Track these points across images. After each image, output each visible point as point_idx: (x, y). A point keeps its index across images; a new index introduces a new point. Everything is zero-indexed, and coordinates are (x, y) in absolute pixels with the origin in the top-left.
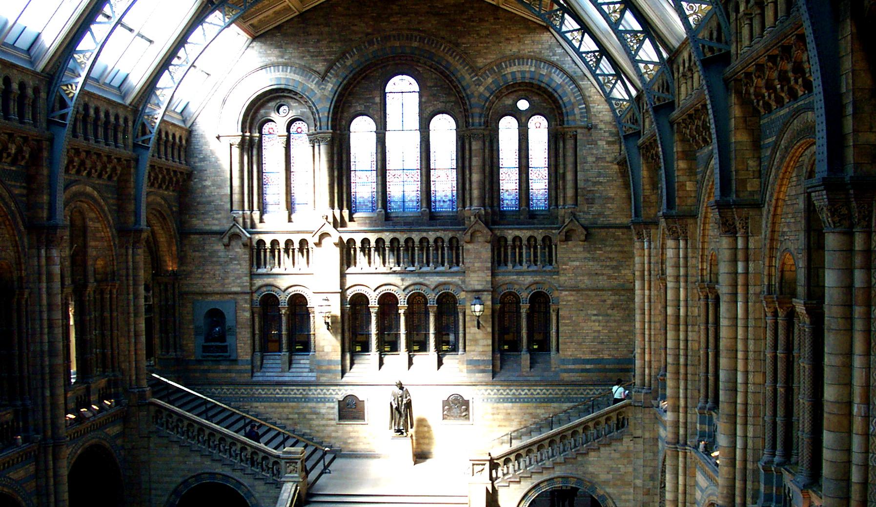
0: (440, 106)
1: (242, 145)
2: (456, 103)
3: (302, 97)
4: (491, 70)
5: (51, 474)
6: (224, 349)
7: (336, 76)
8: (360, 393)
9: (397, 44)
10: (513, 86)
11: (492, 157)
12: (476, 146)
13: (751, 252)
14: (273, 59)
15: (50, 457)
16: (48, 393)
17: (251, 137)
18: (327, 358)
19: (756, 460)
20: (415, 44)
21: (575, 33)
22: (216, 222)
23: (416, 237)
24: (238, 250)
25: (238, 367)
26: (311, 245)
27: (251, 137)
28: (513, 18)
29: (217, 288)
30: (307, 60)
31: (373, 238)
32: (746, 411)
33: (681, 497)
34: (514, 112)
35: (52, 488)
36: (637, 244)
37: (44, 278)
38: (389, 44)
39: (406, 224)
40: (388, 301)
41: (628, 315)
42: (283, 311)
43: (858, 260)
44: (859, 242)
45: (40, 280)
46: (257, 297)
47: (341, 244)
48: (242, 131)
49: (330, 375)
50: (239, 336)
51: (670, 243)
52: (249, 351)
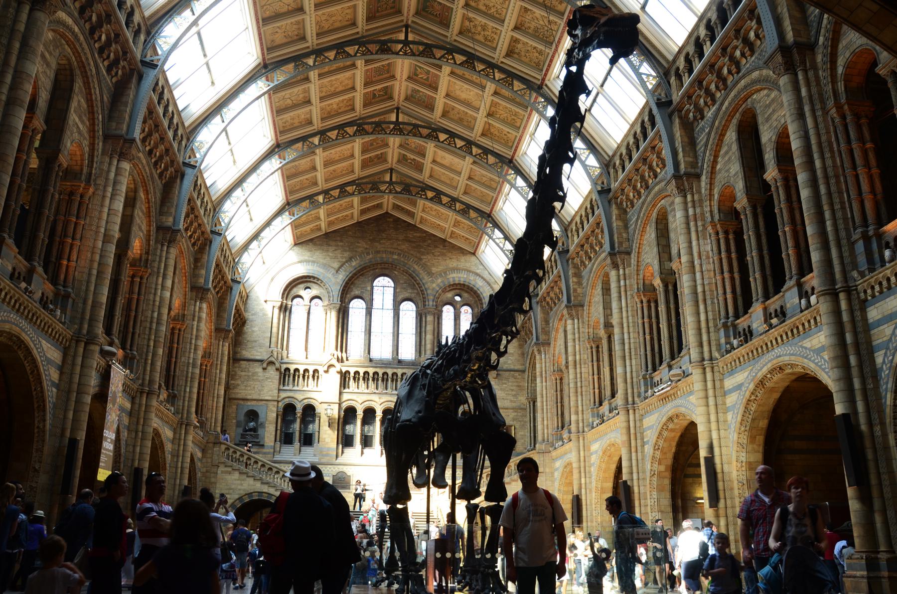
0: (407, 295)
1: (280, 308)
2: (418, 294)
3: (322, 282)
4: (441, 275)
5: (182, 442)
6: (257, 436)
7: (345, 271)
8: (349, 471)
9: (384, 256)
10: (453, 285)
11: (438, 327)
12: (430, 318)
13: (627, 275)
14: (306, 258)
15: (183, 432)
16: (188, 390)
17: (286, 304)
18: (327, 446)
19: (638, 376)
20: (395, 257)
21: (501, 240)
22: (259, 354)
23: (390, 372)
24: (272, 372)
25: (264, 450)
26: (321, 372)
27: (286, 304)
28: (454, 248)
29: (254, 397)
30: (327, 261)
31: (362, 371)
32: (630, 353)
33: (582, 464)
34: (451, 303)
35: (181, 452)
36: (538, 357)
37: (196, 319)
38: (379, 255)
39: (383, 364)
40: (369, 413)
41: (523, 425)
42: (299, 415)
43: (690, 205)
44: (689, 198)
45: (193, 320)
46: (281, 405)
47: (340, 372)
48: (282, 298)
49: (328, 458)
50: (267, 429)
51: (569, 322)
52: (273, 439)
